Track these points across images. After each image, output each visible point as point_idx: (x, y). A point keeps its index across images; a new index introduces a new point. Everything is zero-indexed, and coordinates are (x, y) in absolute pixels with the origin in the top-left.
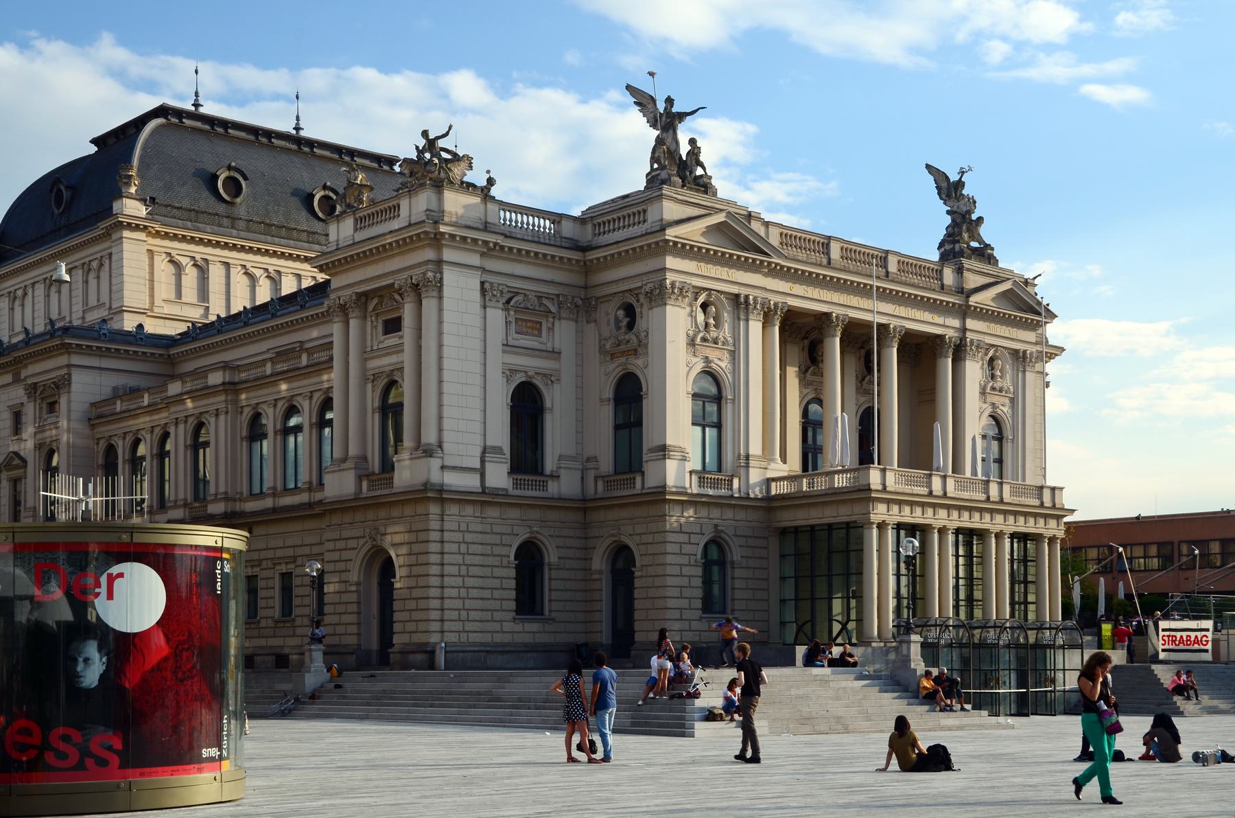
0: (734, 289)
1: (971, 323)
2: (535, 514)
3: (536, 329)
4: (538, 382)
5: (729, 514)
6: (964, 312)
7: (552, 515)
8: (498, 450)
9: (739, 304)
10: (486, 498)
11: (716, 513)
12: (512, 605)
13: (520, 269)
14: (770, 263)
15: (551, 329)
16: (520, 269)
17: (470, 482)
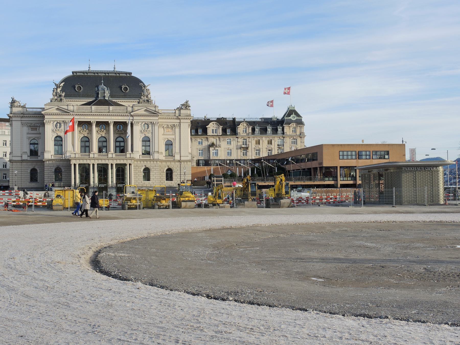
0: (63, 120)
1: (135, 118)
2: (35, 163)
3: (36, 129)
4: (36, 139)
5: (61, 162)
6: (132, 116)
7: (38, 163)
8: (26, 152)
10: (22, 161)
11: (58, 162)
12: (29, 180)
13: (30, 119)
15: (39, 129)
16: (30, 119)
17: (19, 159)
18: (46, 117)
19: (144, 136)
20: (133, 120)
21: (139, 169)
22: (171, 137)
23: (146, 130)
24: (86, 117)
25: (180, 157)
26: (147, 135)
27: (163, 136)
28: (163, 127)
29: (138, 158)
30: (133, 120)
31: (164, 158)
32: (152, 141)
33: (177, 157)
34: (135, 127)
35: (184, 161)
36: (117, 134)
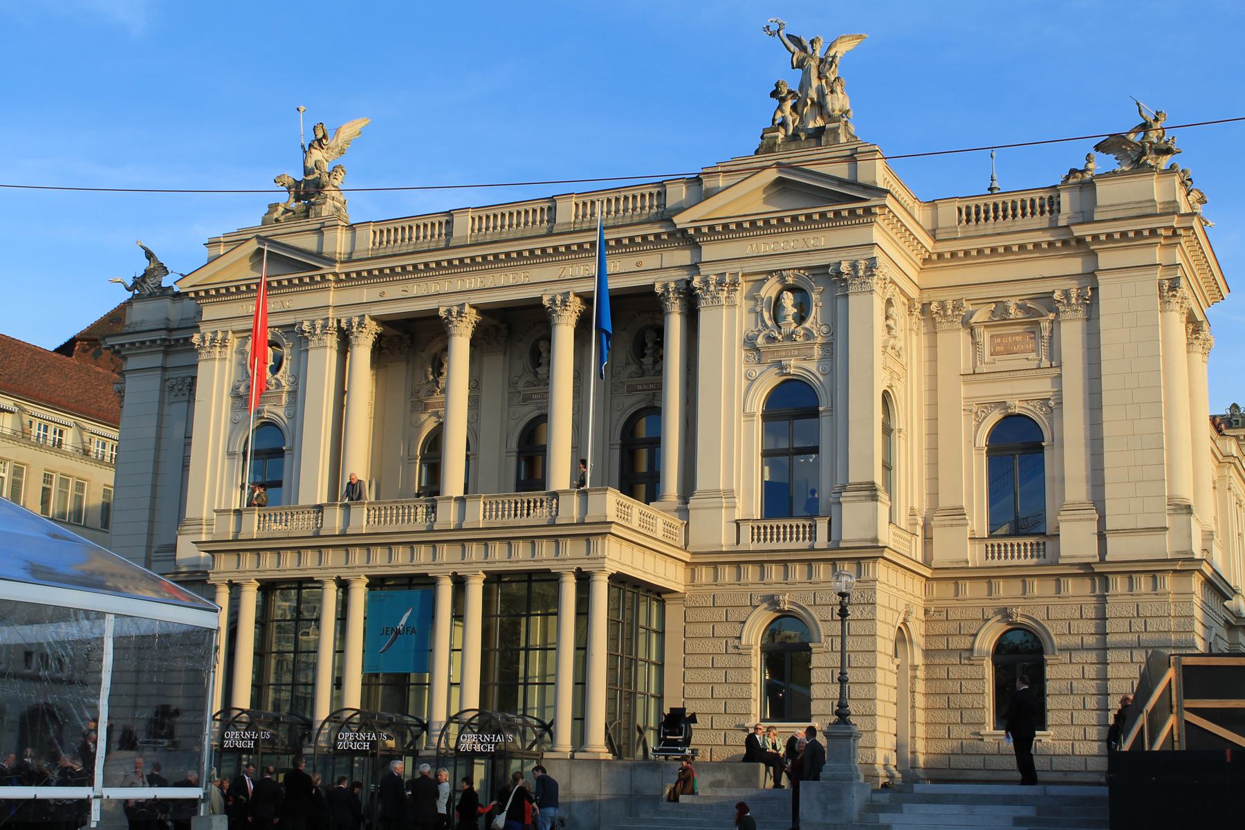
0: (288, 319)
9: (298, 337)
14: (323, 276)
18: (209, 312)
19: (771, 380)
20: (694, 267)
21: (730, 630)
22: (1022, 395)
23: (789, 324)
24: (415, 289)
25: (1102, 537)
26: (794, 366)
27: (963, 391)
28: (966, 323)
29: (725, 539)
30: (694, 267)
31: (974, 555)
32: (831, 410)
33: (1076, 540)
34: (706, 317)
35: (1131, 571)
36: (632, 389)
